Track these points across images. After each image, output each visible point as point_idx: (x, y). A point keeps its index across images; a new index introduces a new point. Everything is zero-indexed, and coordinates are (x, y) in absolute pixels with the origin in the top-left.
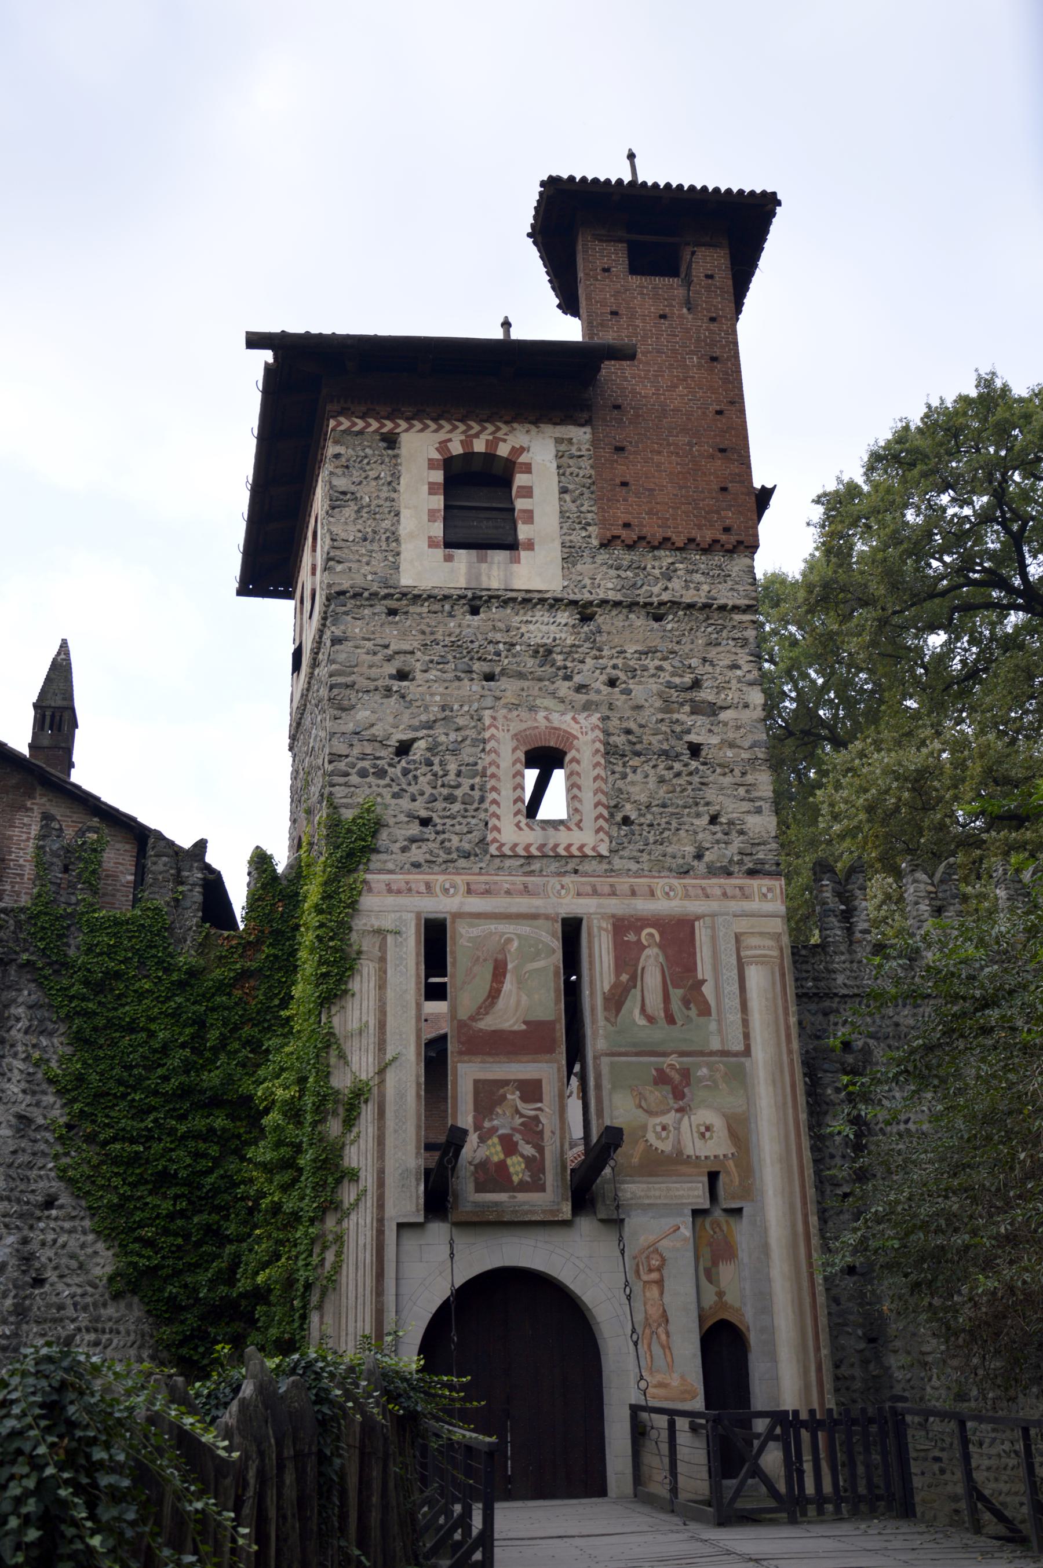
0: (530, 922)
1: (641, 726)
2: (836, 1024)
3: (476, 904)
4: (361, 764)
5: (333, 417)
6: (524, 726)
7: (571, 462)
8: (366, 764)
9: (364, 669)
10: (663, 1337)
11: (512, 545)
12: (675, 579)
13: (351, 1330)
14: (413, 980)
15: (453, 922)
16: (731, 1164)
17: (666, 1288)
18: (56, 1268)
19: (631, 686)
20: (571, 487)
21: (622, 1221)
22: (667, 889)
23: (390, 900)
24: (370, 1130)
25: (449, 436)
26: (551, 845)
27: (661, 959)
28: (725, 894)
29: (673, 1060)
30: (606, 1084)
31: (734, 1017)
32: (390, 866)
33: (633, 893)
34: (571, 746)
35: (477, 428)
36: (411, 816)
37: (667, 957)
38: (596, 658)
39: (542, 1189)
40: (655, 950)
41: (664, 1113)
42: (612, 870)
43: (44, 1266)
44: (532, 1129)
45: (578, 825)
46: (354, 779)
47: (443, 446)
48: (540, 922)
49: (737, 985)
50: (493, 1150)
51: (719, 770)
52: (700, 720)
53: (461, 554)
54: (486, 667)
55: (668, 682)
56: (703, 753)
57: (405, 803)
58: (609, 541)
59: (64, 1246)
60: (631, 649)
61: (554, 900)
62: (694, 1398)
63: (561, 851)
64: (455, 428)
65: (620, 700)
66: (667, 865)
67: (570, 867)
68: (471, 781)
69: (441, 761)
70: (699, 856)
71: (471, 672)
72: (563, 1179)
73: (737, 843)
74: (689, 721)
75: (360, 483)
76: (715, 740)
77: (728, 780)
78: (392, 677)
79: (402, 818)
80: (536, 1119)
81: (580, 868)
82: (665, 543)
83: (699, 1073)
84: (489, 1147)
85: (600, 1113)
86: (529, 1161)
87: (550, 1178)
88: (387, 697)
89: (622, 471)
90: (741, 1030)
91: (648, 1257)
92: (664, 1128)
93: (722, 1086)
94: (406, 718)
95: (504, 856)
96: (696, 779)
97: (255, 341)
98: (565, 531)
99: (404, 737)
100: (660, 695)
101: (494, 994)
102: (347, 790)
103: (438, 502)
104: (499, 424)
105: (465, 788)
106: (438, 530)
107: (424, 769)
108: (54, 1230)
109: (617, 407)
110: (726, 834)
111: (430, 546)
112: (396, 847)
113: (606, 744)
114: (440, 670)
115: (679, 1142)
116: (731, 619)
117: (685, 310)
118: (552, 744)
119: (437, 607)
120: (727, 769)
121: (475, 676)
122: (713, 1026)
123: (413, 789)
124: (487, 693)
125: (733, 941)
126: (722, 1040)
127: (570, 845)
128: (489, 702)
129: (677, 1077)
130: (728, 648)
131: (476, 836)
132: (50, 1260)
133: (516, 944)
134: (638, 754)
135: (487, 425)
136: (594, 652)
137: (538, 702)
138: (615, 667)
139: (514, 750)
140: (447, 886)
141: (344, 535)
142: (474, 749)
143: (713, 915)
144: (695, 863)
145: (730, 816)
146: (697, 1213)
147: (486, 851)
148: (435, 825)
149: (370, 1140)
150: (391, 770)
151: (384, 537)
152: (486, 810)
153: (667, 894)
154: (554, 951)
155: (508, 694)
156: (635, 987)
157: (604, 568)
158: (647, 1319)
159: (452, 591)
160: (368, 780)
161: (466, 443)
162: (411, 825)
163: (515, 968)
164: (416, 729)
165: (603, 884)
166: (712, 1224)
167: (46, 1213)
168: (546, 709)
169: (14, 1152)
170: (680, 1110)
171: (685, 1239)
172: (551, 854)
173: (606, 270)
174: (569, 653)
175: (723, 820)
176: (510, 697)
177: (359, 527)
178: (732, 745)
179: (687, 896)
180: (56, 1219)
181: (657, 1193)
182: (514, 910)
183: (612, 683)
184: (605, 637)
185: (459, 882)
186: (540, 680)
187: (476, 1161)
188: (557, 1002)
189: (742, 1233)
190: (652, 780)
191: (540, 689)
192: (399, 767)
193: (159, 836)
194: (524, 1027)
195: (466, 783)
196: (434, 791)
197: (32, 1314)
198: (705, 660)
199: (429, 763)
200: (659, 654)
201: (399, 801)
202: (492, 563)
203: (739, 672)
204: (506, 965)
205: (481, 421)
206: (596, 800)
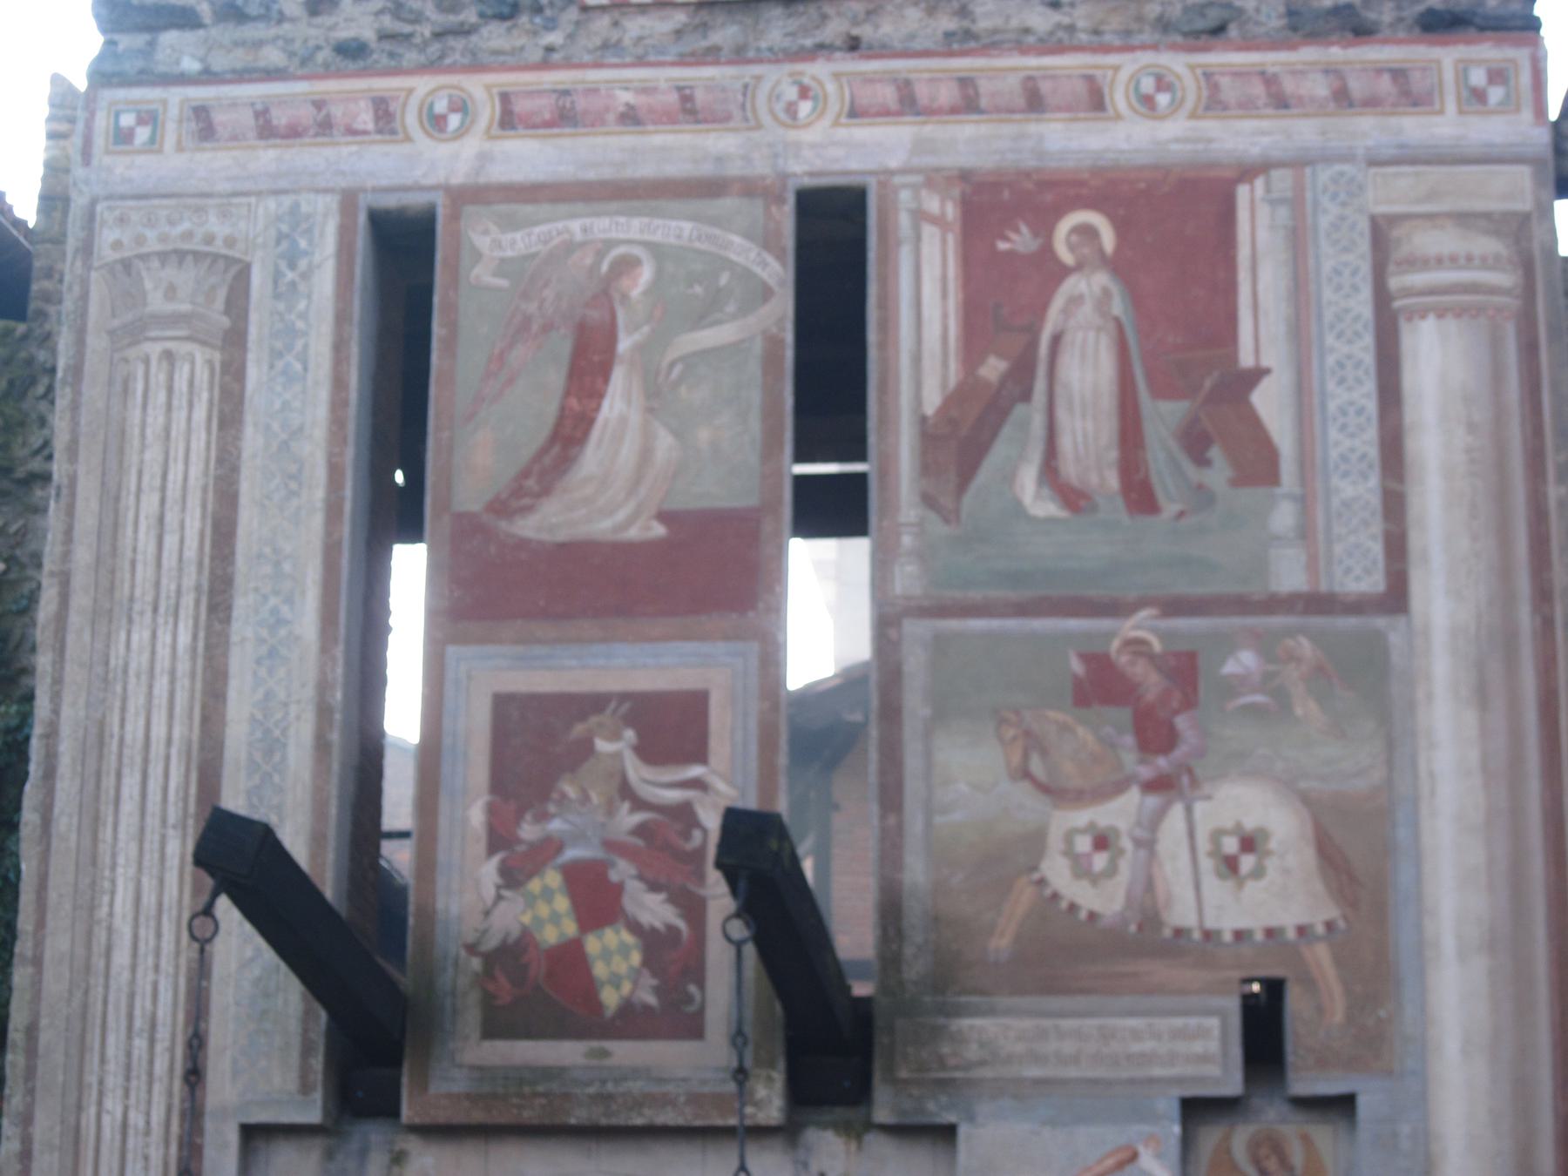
14: (324, 394)
15: (455, 216)
16: (1321, 956)
21: (947, 1133)
22: (1148, 85)
23: (267, 158)
27: (1118, 307)
29: (1141, 625)
31: (1364, 489)
32: (273, 56)
33: (1034, 101)
37: (1136, 299)
39: (693, 1028)
40: (1101, 279)
48: (728, 203)
49: (1370, 385)
50: (543, 910)
81: (865, 32)
83: (1230, 668)
84: (531, 901)
86: (655, 943)
90: (1377, 527)
92: (1102, 842)
93: (1305, 707)
115: (1150, 886)
122: (1284, 517)
125: (1364, 246)
126: (1312, 565)
129: (1151, 682)
133: (646, 274)
140: (441, 106)
143: (1299, 163)
146: (1196, 1110)
153: (1148, 101)
154: (767, 293)
156: (1026, 396)
163: (639, 348)
166: (1254, 1146)
170: (1160, 785)
179: (1214, 104)
181: (1069, 1047)
182: (646, 170)
187: (492, 943)
194: (659, 530)
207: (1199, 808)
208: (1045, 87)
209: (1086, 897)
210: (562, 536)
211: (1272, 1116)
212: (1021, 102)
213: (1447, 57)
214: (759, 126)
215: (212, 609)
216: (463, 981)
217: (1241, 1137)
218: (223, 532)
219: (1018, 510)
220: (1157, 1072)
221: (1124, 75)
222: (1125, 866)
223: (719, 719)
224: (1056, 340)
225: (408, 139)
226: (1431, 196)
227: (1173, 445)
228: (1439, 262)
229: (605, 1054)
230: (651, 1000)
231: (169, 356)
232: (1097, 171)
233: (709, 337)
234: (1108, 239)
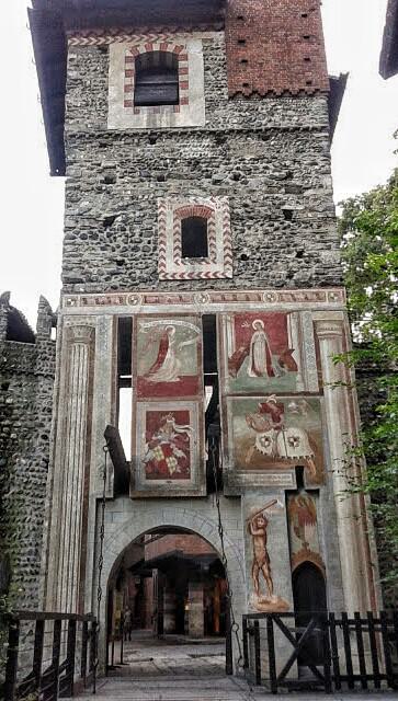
3: (149, 309)
8: (85, 232)
9: (86, 178)
10: (266, 571)
23: (98, 308)
24: (82, 442)
28: (306, 298)
30: (229, 413)
31: (312, 372)
32: (99, 289)
33: (248, 299)
34: (210, 216)
36: (112, 260)
38: (226, 164)
40: (262, 332)
41: (266, 430)
44: (182, 441)
46: (79, 240)
48: (189, 318)
52: (291, 196)
54: (158, 173)
57: (108, 253)
60: (248, 157)
70: (290, 277)
73: (314, 268)
78: (102, 182)
80: (185, 435)
86: (180, 460)
87: (193, 470)
89: (242, 54)
92: (267, 440)
96: (288, 231)
99: (108, 215)
101: (160, 361)
102: (73, 247)
103: (131, 81)
106: (131, 96)
119: (129, 141)
120: (308, 224)
122: (298, 377)
123: (112, 245)
133: (174, 331)
134: (252, 218)
138: (238, 169)
144: (288, 281)
146: (288, 492)
150: (100, 234)
158: (255, 559)
163: (175, 345)
164: (116, 211)
165: (228, 295)
168: (195, 195)
175: (305, 254)
178: (311, 210)
182: (172, 311)
183: (236, 178)
188: (199, 362)
189: (319, 505)
194: (178, 380)
195: (146, 240)
198: (295, 161)
203: (316, 167)
213: (326, 291)
218: (91, 381)
233: (189, 342)
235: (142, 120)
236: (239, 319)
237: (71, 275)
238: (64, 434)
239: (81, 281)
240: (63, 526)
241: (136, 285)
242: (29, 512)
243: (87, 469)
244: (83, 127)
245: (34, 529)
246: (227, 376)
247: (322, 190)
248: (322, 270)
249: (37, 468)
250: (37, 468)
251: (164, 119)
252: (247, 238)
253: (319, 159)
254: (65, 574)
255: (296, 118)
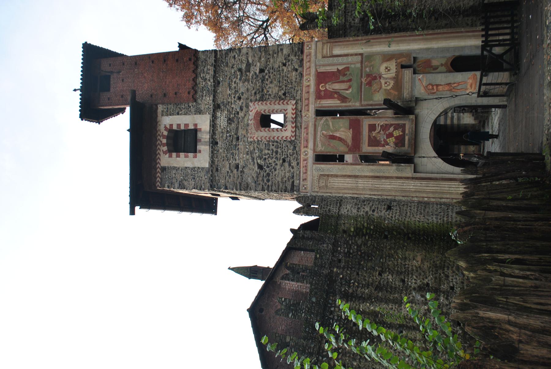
0: (317, 127)
1: (254, 89)
2: (354, 23)
3: (311, 145)
4: (265, 181)
5: (156, 187)
6: (253, 128)
7: (169, 111)
8: (265, 180)
9: (235, 179)
10: (455, 85)
11: (195, 131)
12: (206, 77)
13: (448, 189)
14: (335, 166)
15: (316, 152)
16: (399, 61)
17: (439, 84)
18: (423, 279)
19: (241, 92)
20: (177, 111)
22: (307, 81)
23: (309, 173)
24: (383, 181)
25: (161, 151)
26: (292, 120)
27: (330, 83)
28: (309, 61)
29: (363, 80)
30: (371, 102)
31: (350, 59)
32: (298, 172)
33: (308, 92)
35: (159, 142)
36: (282, 166)
37: (329, 82)
38: (231, 104)
39: (405, 125)
40: (327, 85)
41: (381, 83)
42: (301, 99)
43: (423, 283)
44: (385, 128)
45: (285, 110)
46: (270, 183)
47: (165, 153)
48: (317, 124)
49: (339, 58)
50: (391, 141)
51: (268, 63)
52: (252, 68)
53: (199, 147)
54: (234, 140)
55: (239, 80)
56: (263, 68)
57: (278, 167)
58: (194, 99)
59: (417, 277)
60: (229, 92)
61: (310, 119)
62: (476, 75)
63: (294, 116)
64: (159, 149)
65: (245, 96)
66: (299, 81)
67: (299, 113)
68: (271, 145)
69: (264, 155)
71: (236, 145)
72: (402, 117)
73: (292, 57)
74: (252, 73)
75: (177, 180)
76: (258, 64)
77: (272, 60)
78: (237, 171)
79: (282, 168)
80: (382, 126)
81: (299, 110)
82: (195, 80)
83: (368, 71)
84: (390, 142)
85: (380, 105)
86: (395, 129)
88: (244, 172)
90: (354, 57)
91: (428, 90)
93: (373, 63)
94: (251, 166)
95: (295, 135)
96: (271, 71)
97: (132, 212)
98: (191, 114)
99: (257, 167)
100: (244, 83)
101: (340, 139)
102: (273, 186)
103: (182, 155)
104: (157, 135)
105: (273, 147)
106: (191, 155)
107: (267, 161)
108: (411, 280)
109: (151, 96)
110: (289, 61)
111: (196, 158)
112: (292, 171)
113: (259, 101)
114: (235, 155)
115: (391, 78)
116: (219, 58)
117: (121, 73)
118: (259, 119)
119: (215, 156)
120: (268, 60)
121: (237, 144)
122: (353, 66)
123: (273, 165)
124: (243, 140)
125: (325, 59)
126: (357, 63)
127: (292, 113)
128: (245, 139)
129: (369, 79)
130: (228, 59)
131: (289, 145)
132: (421, 281)
133: (324, 132)
134: (263, 90)
135: (158, 138)
136: (230, 104)
137: (245, 123)
138: (234, 97)
139: (261, 131)
140: (305, 154)
141: (193, 185)
142: (261, 144)
143: (316, 66)
144: (299, 71)
145: (283, 59)
146: (415, 72)
147: (294, 141)
148: (285, 157)
149: (386, 181)
150: (267, 171)
151: (193, 172)
152: (280, 141)
154: (327, 119)
155: (243, 133)
156: (339, 92)
157: (203, 101)
158: (449, 90)
159: (210, 151)
160: (270, 179)
161: (164, 145)
162: (285, 165)
163: (332, 132)
164: (254, 163)
165: (305, 102)
167: (406, 282)
168: (248, 120)
169: (387, 292)
170: (380, 78)
171: (423, 77)
172: (295, 119)
173: (109, 99)
174: (230, 113)
175: (285, 61)
176: (244, 132)
177: (190, 180)
178: (260, 58)
179: (309, 74)
180: (408, 279)
181: (407, 86)
182: (313, 132)
183: (239, 98)
184: (225, 101)
185: (303, 150)
186: (239, 122)
187: (395, 146)
189: (422, 57)
190: (271, 85)
191: (242, 122)
192: (266, 169)
193: (289, 244)
194: (351, 130)
195: (271, 147)
196: (274, 157)
197: (437, 287)
198: (232, 67)
199: (265, 159)
200: (230, 83)
201: (277, 169)
202: (201, 137)
203: (236, 56)
204: (331, 135)
205: (157, 141)
206: (277, 104)
207: (383, 73)
208: (306, 91)
209: (392, 84)
210: (351, 140)
211: (415, 65)
212: (308, 94)
213: (306, 51)
214: (309, 120)
215: (357, 177)
216: (399, 149)
217: (418, 69)
218: (349, 176)
219: (351, 93)
220: (410, 77)
221: (306, 83)
222: (388, 81)
223: (371, 123)
224: (333, 89)
225: (308, 157)
226: (320, 52)
227: (345, 77)
228: (327, 51)
229: (407, 134)
230: (401, 129)
231: (330, 182)
232: (316, 86)
234: (323, 84)
235: (204, 149)
236: (319, 96)
237: (289, 188)
238: (378, 191)
239: (293, 182)
240: (427, 190)
241: (297, 152)
242: (414, 219)
243: (398, 178)
244: (207, 180)
245: (424, 216)
246: (350, 104)
247: (249, 53)
248: (294, 53)
249: (391, 215)
250: (391, 215)
251: (204, 136)
252: (274, 92)
253: (232, 54)
254: (452, 189)
255: (209, 67)
